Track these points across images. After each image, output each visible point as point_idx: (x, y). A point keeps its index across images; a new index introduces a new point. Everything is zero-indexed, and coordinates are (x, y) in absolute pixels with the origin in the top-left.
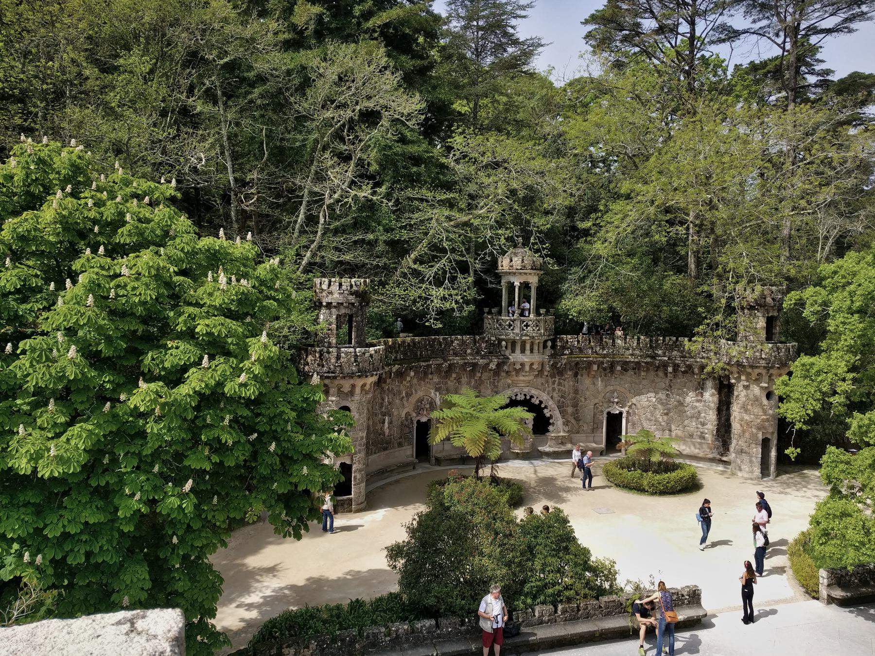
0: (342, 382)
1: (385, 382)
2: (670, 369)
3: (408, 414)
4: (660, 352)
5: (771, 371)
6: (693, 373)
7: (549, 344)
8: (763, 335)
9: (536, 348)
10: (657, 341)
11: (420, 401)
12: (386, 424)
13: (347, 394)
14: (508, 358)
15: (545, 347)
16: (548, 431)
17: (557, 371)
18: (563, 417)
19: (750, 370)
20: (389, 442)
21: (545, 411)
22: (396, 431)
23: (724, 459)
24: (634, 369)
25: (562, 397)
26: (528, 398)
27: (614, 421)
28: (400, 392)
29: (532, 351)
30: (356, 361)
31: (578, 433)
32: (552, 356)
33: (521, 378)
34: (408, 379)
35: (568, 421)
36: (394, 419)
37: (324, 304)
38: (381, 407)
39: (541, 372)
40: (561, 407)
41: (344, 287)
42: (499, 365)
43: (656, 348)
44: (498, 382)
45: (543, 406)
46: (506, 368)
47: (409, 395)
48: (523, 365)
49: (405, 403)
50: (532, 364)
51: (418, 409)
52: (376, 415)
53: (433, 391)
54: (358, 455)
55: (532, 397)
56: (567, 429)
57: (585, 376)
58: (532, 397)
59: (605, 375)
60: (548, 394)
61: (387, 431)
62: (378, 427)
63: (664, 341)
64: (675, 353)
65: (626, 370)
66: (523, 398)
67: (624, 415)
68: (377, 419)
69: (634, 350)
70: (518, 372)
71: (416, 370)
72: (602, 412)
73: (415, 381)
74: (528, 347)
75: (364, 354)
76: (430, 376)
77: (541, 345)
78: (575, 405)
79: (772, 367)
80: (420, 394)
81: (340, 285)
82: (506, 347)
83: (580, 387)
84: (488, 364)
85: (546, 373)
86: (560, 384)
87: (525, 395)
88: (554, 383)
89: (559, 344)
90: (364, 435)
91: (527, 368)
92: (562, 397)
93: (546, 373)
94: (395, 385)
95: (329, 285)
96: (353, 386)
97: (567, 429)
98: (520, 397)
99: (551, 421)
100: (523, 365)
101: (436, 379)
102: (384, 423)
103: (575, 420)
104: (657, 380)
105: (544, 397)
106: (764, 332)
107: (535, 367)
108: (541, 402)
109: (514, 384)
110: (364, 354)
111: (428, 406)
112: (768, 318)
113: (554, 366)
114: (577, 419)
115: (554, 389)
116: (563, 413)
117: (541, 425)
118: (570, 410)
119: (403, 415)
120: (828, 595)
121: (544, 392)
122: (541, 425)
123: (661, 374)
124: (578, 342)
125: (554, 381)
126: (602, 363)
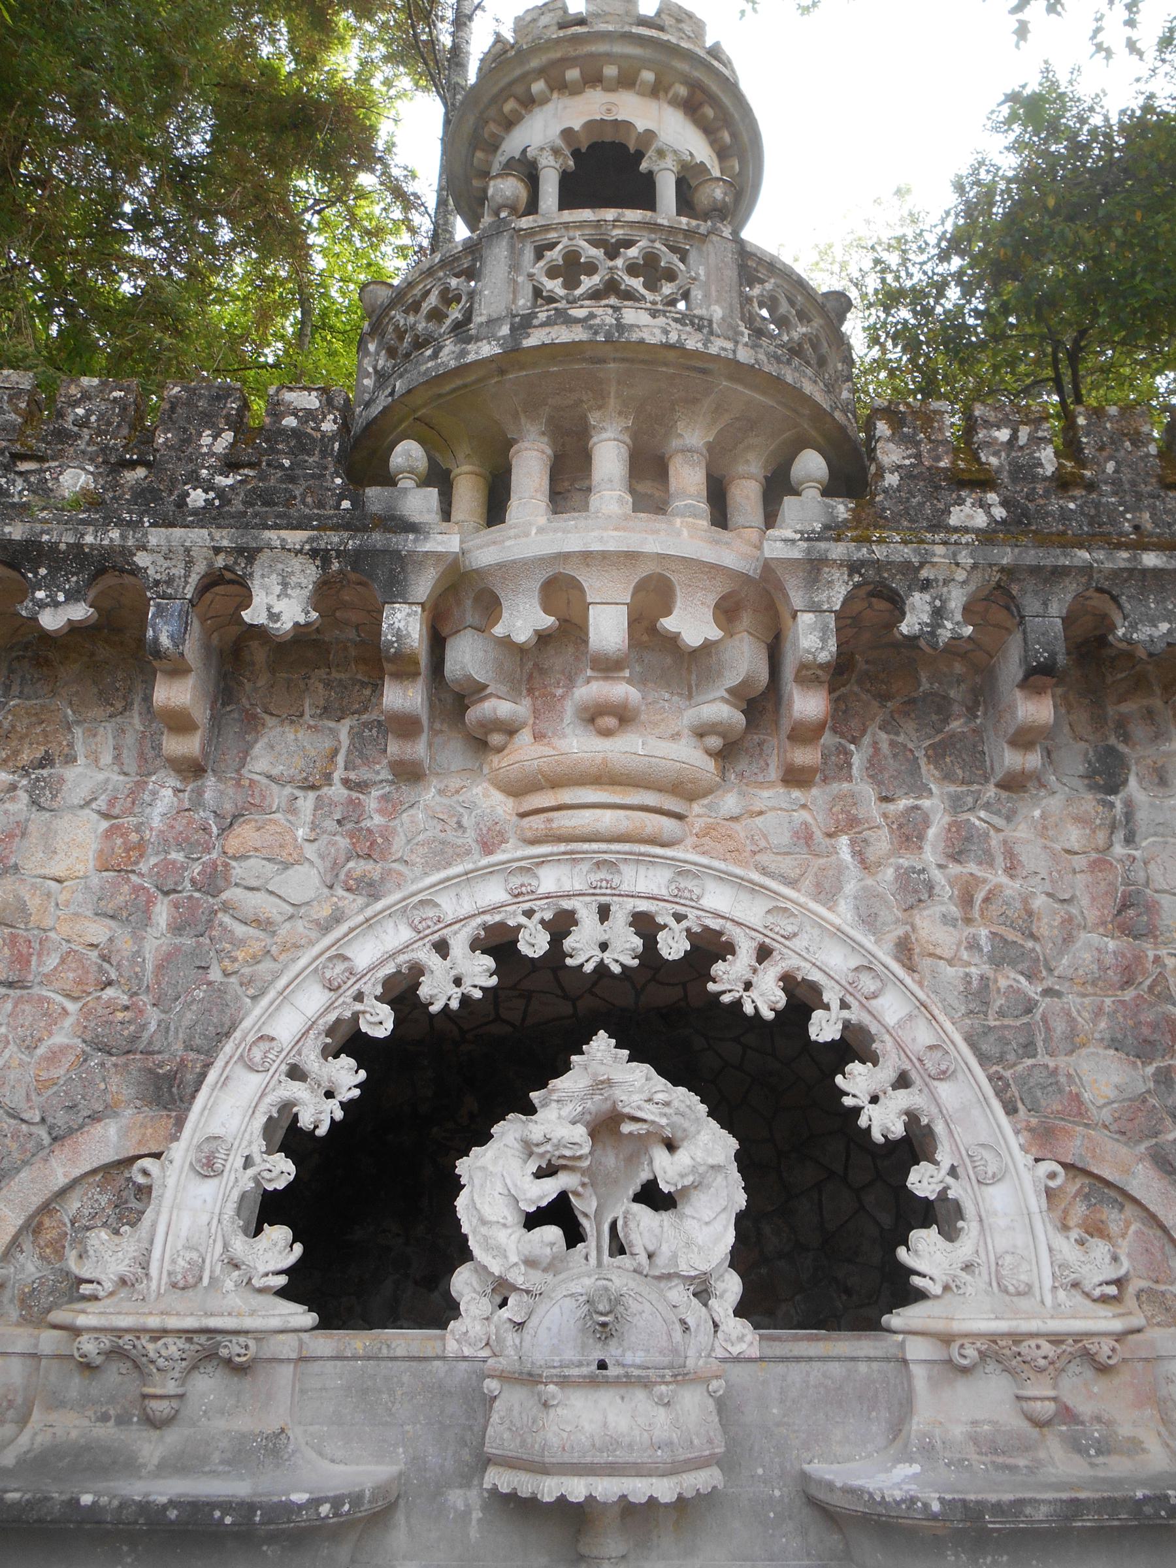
18: (1043, 1138)
21: (856, 1082)
25: (1004, 954)
26: (673, 946)
33: (578, 745)
35: (1104, 1191)
48: (562, 591)
55: (709, 948)
56: (1096, 1265)
58: (709, 948)
60: (869, 920)
66: (625, 948)
87: (645, 925)
88: (909, 833)
91: (608, 628)
92: (1004, 954)
97: (1096, 1265)
98: (602, 946)
99: (923, 1181)
115: (915, 890)
117: (830, 1226)
122: (830, 1226)
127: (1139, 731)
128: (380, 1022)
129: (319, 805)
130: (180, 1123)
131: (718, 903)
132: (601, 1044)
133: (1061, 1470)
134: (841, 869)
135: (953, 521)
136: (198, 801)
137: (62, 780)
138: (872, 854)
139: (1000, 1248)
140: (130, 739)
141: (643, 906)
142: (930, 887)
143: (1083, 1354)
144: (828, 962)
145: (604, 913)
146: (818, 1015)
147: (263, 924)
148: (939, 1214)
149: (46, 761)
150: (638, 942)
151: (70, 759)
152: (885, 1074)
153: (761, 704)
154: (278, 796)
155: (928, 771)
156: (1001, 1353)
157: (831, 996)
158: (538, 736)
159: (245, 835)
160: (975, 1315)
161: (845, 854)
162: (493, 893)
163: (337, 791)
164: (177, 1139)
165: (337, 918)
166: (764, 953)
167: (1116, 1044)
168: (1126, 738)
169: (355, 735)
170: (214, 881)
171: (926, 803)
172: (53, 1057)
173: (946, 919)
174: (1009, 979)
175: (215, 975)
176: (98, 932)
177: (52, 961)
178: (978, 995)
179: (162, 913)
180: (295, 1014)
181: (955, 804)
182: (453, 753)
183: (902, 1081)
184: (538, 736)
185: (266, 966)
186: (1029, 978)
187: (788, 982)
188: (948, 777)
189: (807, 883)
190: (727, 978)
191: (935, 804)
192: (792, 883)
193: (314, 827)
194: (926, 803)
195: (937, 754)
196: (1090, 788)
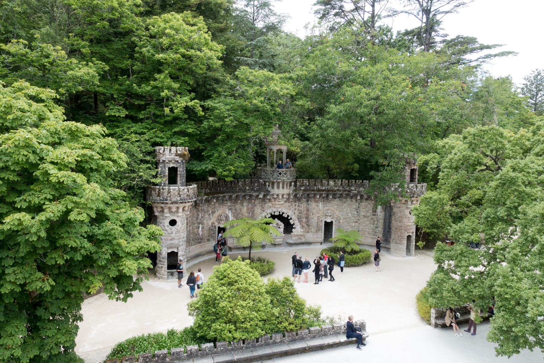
0: (171, 205)
1: (199, 206)
2: (359, 198)
3: (213, 223)
4: (353, 188)
5: (412, 199)
6: (371, 200)
7: (293, 184)
8: (408, 179)
9: (285, 186)
10: (352, 182)
11: (220, 216)
12: (200, 229)
13: (174, 213)
14: (270, 192)
15: (290, 185)
16: (292, 232)
17: (297, 198)
18: (301, 224)
19: (401, 198)
20: (202, 239)
21: (291, 221)
22: (206, 233)
23: (387, 246)
24: (339, 197)
26: (281, 213)
27: (328, 226)
28: (208, 211)
29: (283, 188)
30: (179, 194)
31: (308, 232)
32: (295, 190)
34: (213, 203)
36: (205, 226)
37: (161, 161)
38: (197, 218)
39: (288, 199)
40: (299, 219)
41: (172, 152)
42: (264, 196)
43: (351, 186)
45: (289, 218)
46: (268, 197)
47: (213, 213)
48: (278, 195)
49: (211, 217)
50: (283, 195)
51: (219, 220)
52: (194, 224)
53: (227, 210)
54: (181, 247)
55: (283, 213)
56: (302, 230)
58: (283, 213)
61: (201, 233)
62: (195, 231)
63: (355, 182)
64: (361, 189)
65: (335, 198)
66: (278, 214)
67: (334, 223)
68: (195, 226)
69: (339, 187)
70: (275, 199)
71: (217, 199)
72: (322, 221)
73: (217, 205)
74: (281, 185)
75: (184, 190)
76: (225, 202)
77: (288, 185)
78: (307, 218)
79: (413, 197)
80: (220, 212)
81: (170, 150)
82: (269, 186)
83: (310, 208)
84: (258, 196)
85: (291, 200)
86: (299, 206)
88: (295, 206)
89: (298, 184)
90: (185, 236)
91: (280, 197)
92: (300, 213)
93: (291, 200)
94: (205, 207)
95: (164, 151)
96: (178, 208)
97: (302, 230)
100: (278, 195)
101: (229, 204)
102: (199, 228)
103: (307, 225)
104: (352, 203)
106: (409, 177)
107: (285, 196)
108: (288, 216)
110: (184, 190)
111: (224, 219)
112: (411, 170)
113: (295, 196)
114: (308, 225)
115: (295, 209)
116: (301, 222)
117: (288, 228)
118: (304, 220)
119: (210, 224)
120: (435, 323)
122: (288, 228)
123: (354, 200)
124: (309, 183)
126: (322, 194)
131: (284, 211)
133: (299, 241)
139: (298, 230)
143: (301, 235)
144: (290, 214)
148: (295, 228)
156: (297, 235)
160: (296, 234)
170: (254, 211)
178: (298, 216)
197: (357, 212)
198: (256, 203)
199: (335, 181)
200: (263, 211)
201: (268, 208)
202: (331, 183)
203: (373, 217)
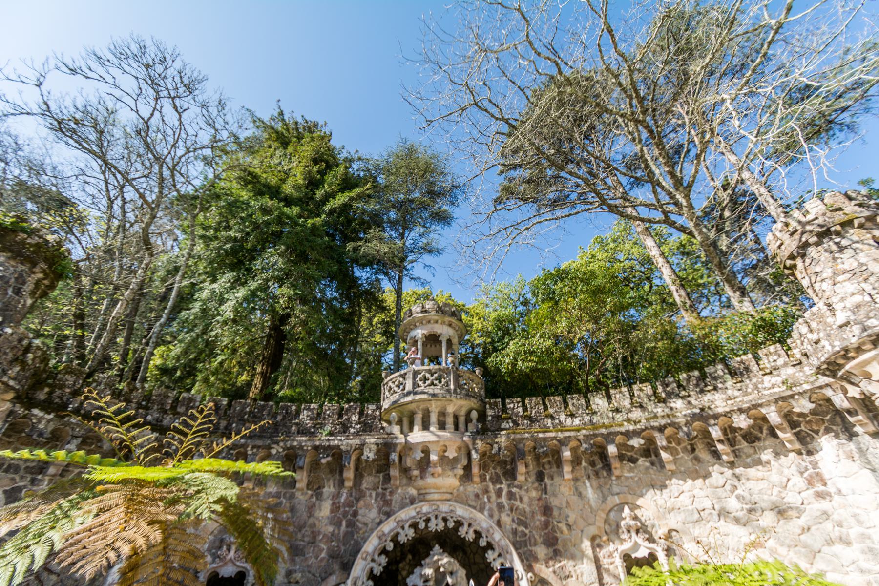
26: (451, 525)
44: (391, 493)
45: (483, 543)
55: (459, 524)
57: (557, 479)
58: (459, 524)
59: (597, 474)
60: (491, 516)
66: (441, 527)
74: (434, 418)
83: (554, 502)
86: (511, 496)
87: (445, 520)
88: (499, 493)
89: (490, 412)
92: (521, 523)
98: (437, 526)
105: (483, 521)
109: (422, 497)
115: (500, 507)
121: (481, 510)
125: (501, 490)
127: (547, 466)
128: (390, 547)
129: (377, 495)
130: (349, 575)
132: (437, 547)
134: (485, 503)
135: (503, 426)
136: (351, 495)
137: (322, 492)
138: (492, 500)
140: (336, 482)
141: (444, 515)
142: (504, 507)
145: (436, 517)
146: (481, 539)
147: (366, 524)
149: (319, 488)
150: (443, 524)
151: (324, 487)
152: (496, 554)
153: (468, 468)
154: (368, 493)
155: (502, 478)
157: (484, 535)
158: (422, 478)
159: (361, 503)
161: (486, 500)
162: (413, 513)
163: (380, 490)
164: (348, 578)
165: (381, 522)
166: (470, 525)
167: (544, 543)
168: (544, 468)
169: (384, 477)
170: (355, 514)
171: (502, 486)
172: (322, 560)
173: (508, 515)
174: (521, 528)
175: (355, 537)
176: (331, 529)
177: (321, 537)
178: (515, 532)
179: (344, 523)
180: (371, 545)
181: (509, 486)
182: (405, 481)
183: (500, 555)
184: (422, 478)
185: (367, 534)
186: (526, 528)
187: (476, 532)
188: (507, 480)
189: (478, 508)
190: (462, 531)
191: (504, 486)
192: (474, 508)
193: (376, 500)
194: (502, 486)
195: (504, 474)
196: (537, 481)
197: (738, 497)
198: (364, 486)
199: (609, 397)
200: (388, 515)
201: (403, 507)
202: (599, 402)
203: (824, 505)
